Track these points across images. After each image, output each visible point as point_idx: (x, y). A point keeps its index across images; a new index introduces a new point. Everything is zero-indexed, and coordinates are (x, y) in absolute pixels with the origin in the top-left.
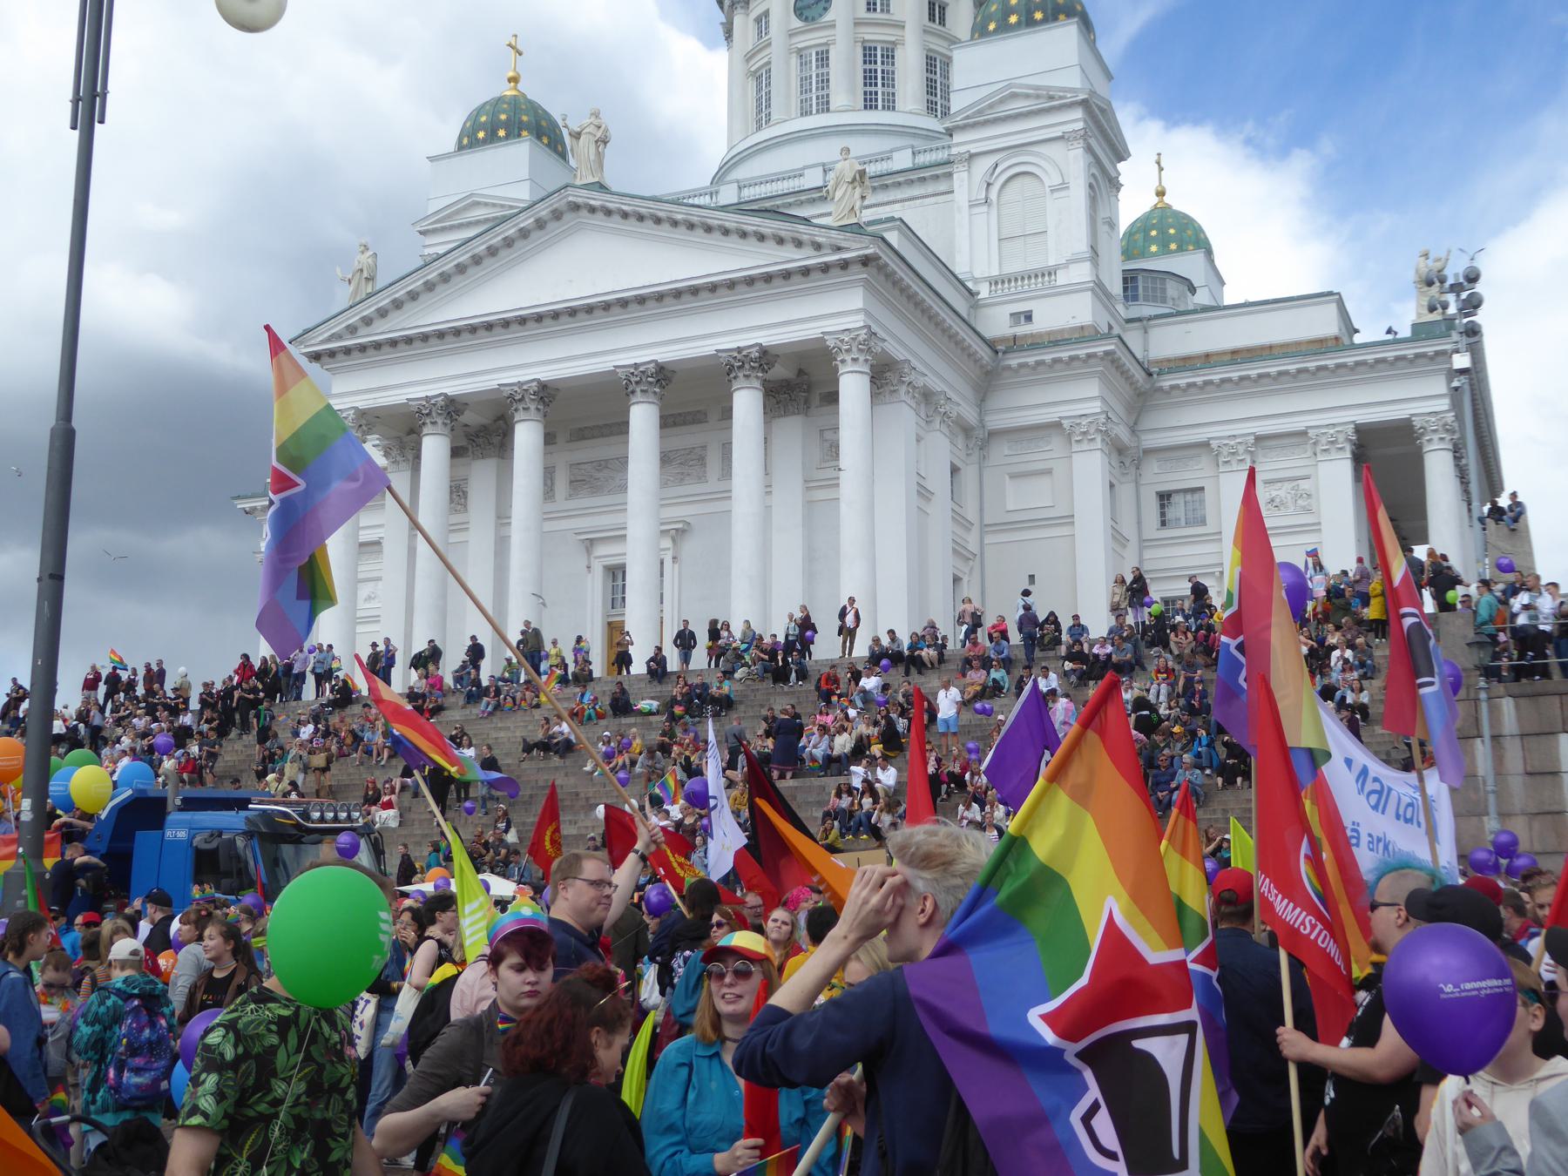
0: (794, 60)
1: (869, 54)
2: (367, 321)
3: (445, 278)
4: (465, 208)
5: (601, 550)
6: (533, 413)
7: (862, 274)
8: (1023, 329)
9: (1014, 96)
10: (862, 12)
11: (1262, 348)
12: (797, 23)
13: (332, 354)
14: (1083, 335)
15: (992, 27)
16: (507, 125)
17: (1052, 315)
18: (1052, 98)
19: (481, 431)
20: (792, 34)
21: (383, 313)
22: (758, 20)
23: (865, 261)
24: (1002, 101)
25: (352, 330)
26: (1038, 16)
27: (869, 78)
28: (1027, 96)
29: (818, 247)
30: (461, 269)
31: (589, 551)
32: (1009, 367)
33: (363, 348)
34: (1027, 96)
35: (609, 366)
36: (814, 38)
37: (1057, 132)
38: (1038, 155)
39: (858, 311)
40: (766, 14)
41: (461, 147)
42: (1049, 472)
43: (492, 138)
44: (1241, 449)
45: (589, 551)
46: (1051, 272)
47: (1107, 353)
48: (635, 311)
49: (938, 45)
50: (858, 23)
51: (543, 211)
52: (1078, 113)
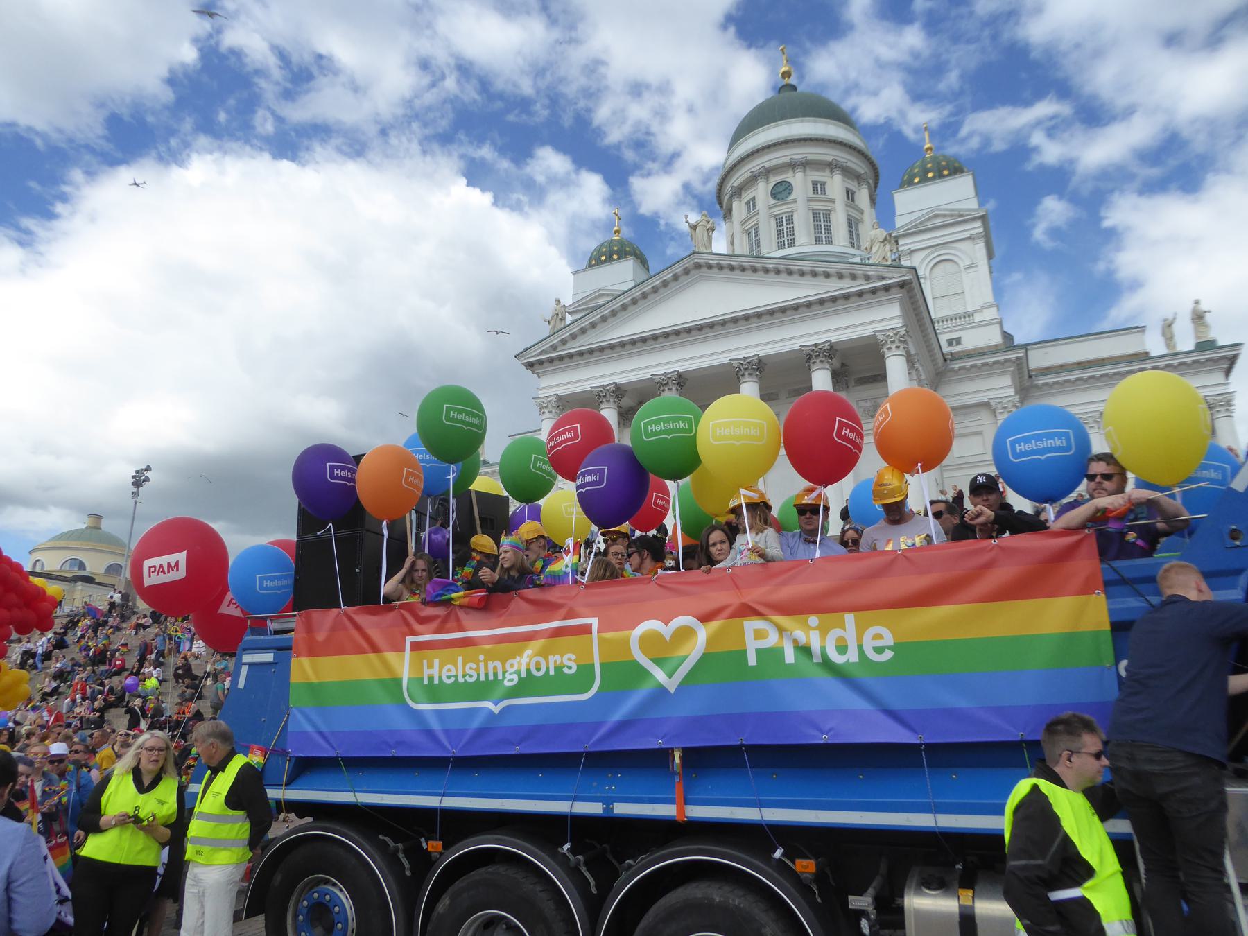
0: (773, 222)
1: (816, 217)
2: (564, 342)
4: (596, 298)
8: (955, 349)
9: (936, 216)
10: (811, 194)
11: (1098, 360)
12: (773, 202)
13: (541, 363)
14: (994, 350)
15: (916, 180)
17: (972, 339)
18: (961, 216)
21: (573, 337)
22: (748, 203)
23: (902, 285)
24: (929, 219)
25: (554, 348)
26: (946, 172)
28: (945, 216)
29: (867, 278)
32: (953, 370)
33: (561, 358)
34: (945, 216)
35: (726, 360)
36: (783, 209)
37: (967, 235)
38: (955, 248)
39: (897, 317)
40: (753, 199)
41: (590, 265)
42: (980, 433)
43: (610, 259)
44: (1091, 420)
46: (970, 315)
47: (1018, 358)
50: (810, 200)
52: (979, 224)
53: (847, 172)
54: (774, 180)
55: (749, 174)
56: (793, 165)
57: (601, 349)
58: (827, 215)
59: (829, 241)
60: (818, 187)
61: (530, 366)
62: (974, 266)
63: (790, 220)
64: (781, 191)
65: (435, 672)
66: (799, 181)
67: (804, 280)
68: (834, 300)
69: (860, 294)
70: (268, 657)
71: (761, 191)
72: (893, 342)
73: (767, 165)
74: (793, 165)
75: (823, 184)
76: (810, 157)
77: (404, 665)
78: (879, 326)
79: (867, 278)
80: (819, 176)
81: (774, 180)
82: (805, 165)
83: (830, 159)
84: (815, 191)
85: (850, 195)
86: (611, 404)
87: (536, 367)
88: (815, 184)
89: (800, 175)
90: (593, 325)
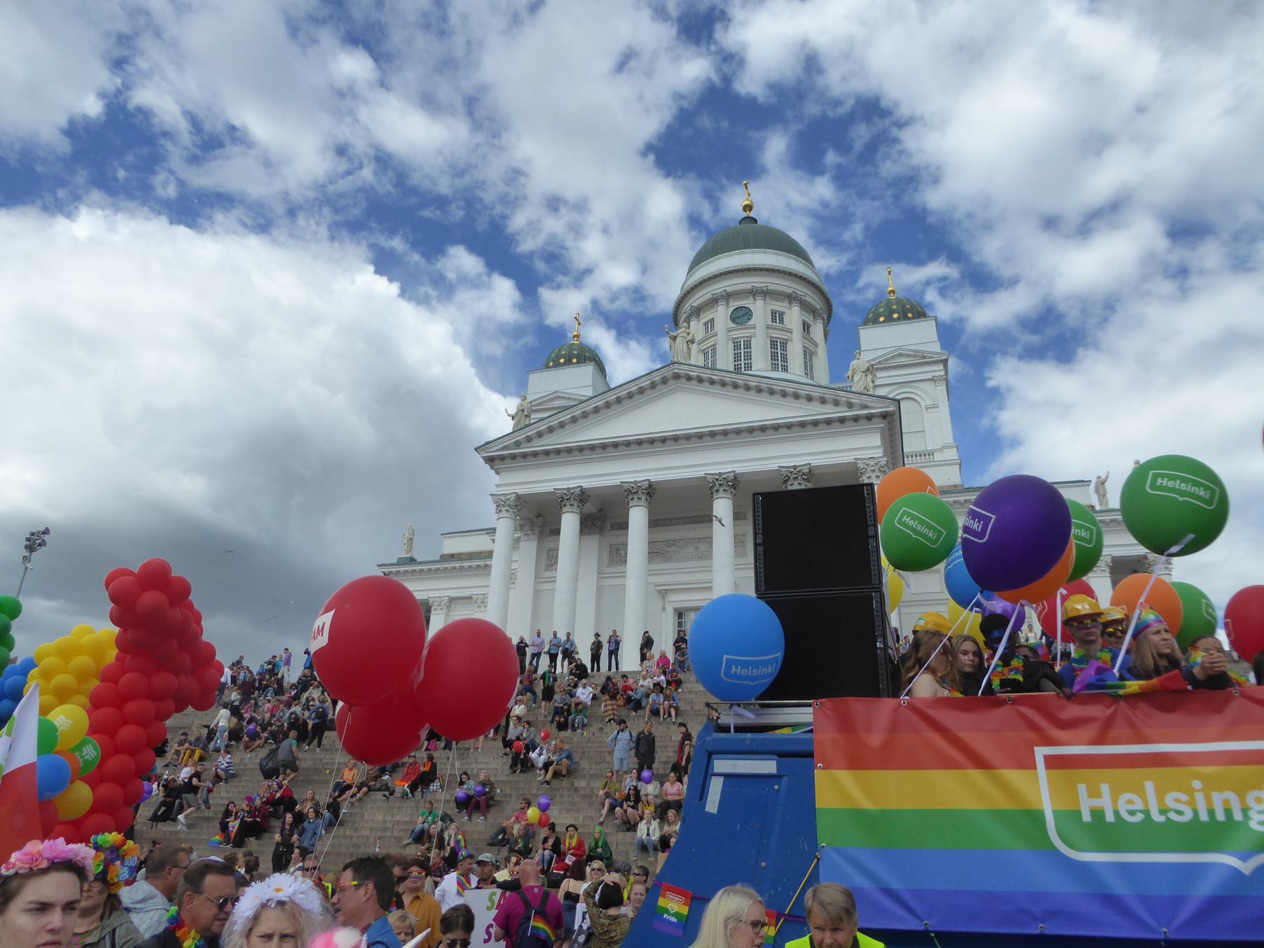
0: (731, 345)
1: (773, 344)
2: (529, 439)
3: (585, 415)
4: (551, 400)
5: (672, 598)
6: (643, 502)
7: (882, 424)
9: (900, 355)
10: (770, 322)
12: (732, 325)
13: (502, 458)
15: (882, 319)
16: (578, 357)
18: (924, 357)
19: (603, 515)
20: (729, 330)
21: (540, 435)
22: (706, 324)
23: (884, 416)
24: (893, 358)
25: (518, 444)
26: (910, 315)
27: (774, 356)
28: (908, 356)
29: (850, 406)
30: (597, 410)
31: (663, 597)
33: (524, 456)
34: (908, 356)
35: (701, 474)
36: (741, 334)
37: (930, 376)
39: (878, 447)
40: (712, 320)
43: (569, 362)
45: (663, 597)
46: (931, 453)
48: (708, 442)
49: (809, 345)
50: (768, 327)
51: (600, 402)
52: (941, 367)
53: (805, 306)
54: (734, 304)
55: (709, 296)
56: (754, 293)
57: (569, 451)
58: (784, 345)
59: (785, 369)
60: (777, 317)
61: (490, 460)
62: (935, 406)
63: (748, 345)
64: (740, 317)
65: (1105, 802)
66: (759, 308)
67: (784, 401)
68: (815, 423)
69: (842, 420)
70: (768, 766)
71: (721, 314)
72: (873, 471)
73: (729, 289)
74: (754, 293)
75: (781, 314)
76: (771, 287)
77: (1040, 788)
78: (859, 454)
79: (850, 406)
80: (779, 306)
81: (734, 304)
82: (766, 294)
83: (790, 291)
84: (774, 320)
85: (806, 327)
86: (575, 509)
87: (497, 462)
88: (773, 313)
89: (760, 302)
90: (562, 425)
